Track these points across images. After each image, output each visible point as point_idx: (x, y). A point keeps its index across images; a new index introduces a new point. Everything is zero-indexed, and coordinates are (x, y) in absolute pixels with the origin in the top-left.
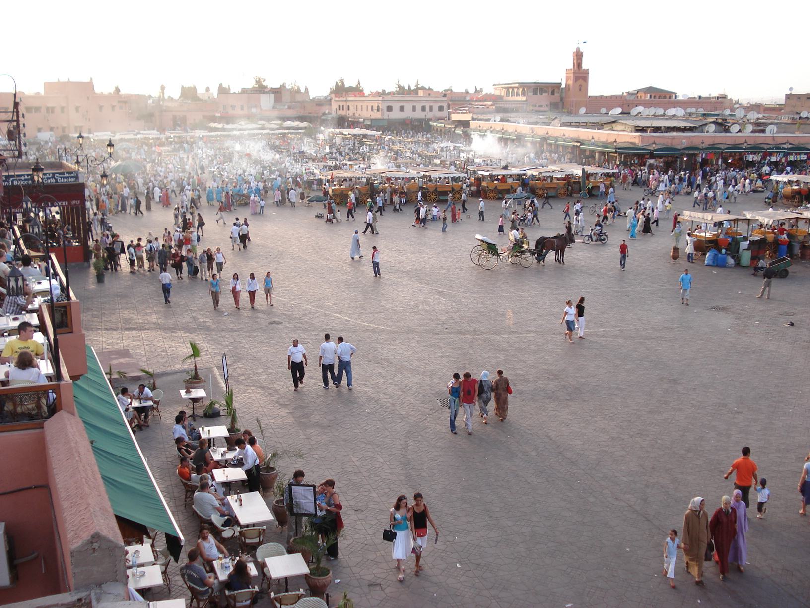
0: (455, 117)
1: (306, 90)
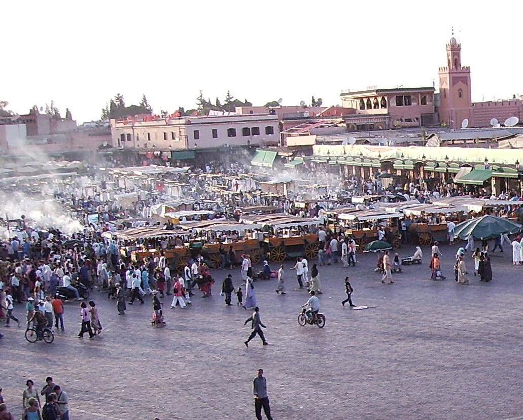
0: (291, 141)
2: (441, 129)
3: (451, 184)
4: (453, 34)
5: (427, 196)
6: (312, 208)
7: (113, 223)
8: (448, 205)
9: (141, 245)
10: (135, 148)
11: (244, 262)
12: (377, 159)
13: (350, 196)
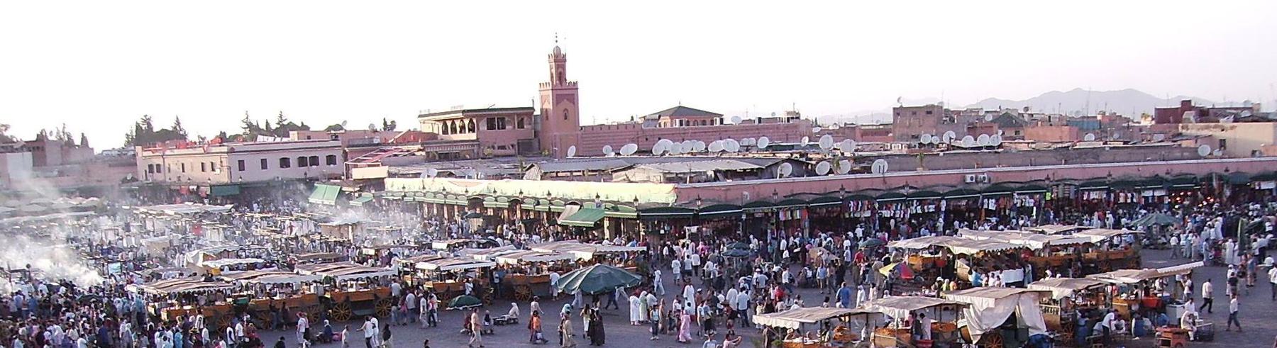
0: (357, 173)
1: (84, 139)
2: (542, 158)
3: (554, 225)
4: (557, 41)
5: (525, 240)
6: (384, 255)
7: (139, 274)
8: (551, 251)
9: (174, 301)
10: (165, 182)
11: (299, 322)
12: (464, 195)
13: (431, 241)
